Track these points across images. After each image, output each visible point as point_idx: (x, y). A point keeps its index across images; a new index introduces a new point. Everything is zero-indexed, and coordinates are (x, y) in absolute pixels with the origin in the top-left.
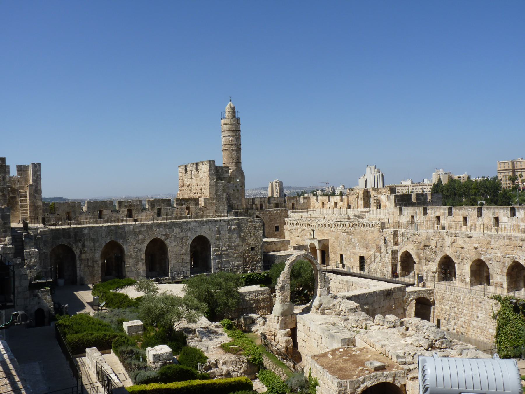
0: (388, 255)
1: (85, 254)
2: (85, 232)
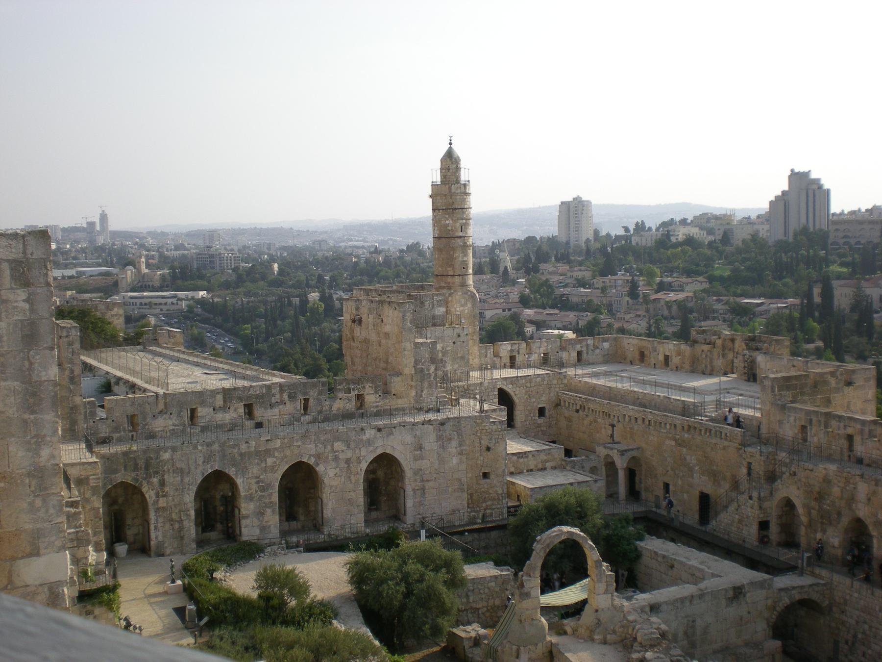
0: (751, 502)
1: (165, 498)
2: (164, 458)
